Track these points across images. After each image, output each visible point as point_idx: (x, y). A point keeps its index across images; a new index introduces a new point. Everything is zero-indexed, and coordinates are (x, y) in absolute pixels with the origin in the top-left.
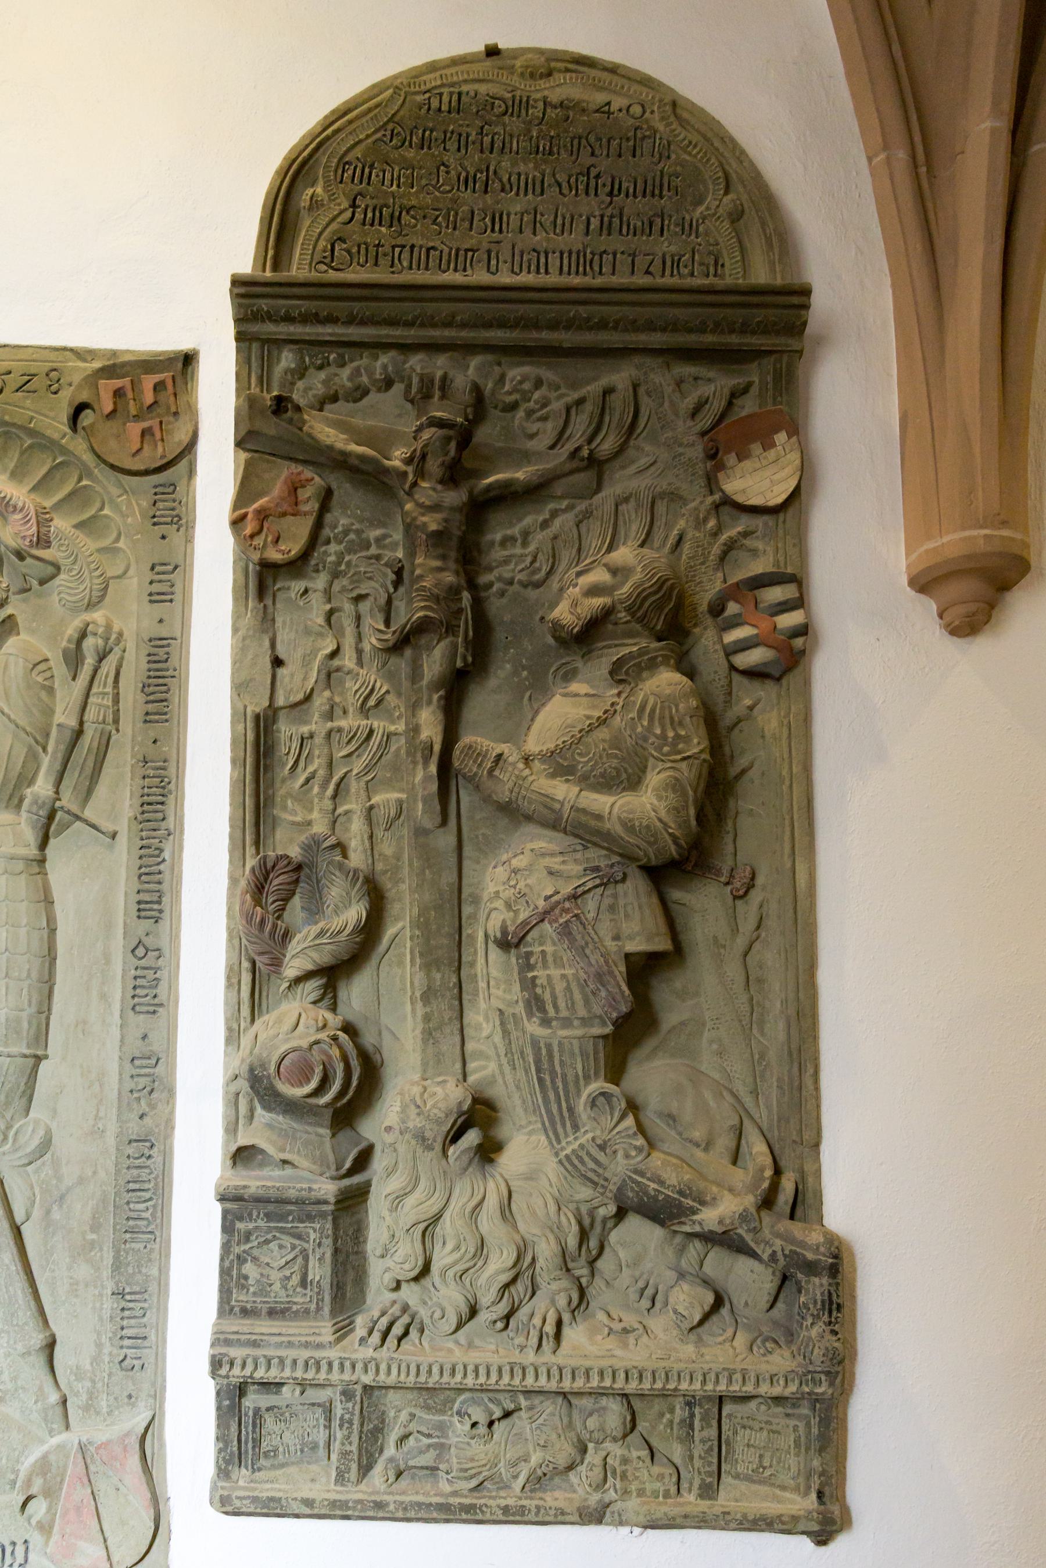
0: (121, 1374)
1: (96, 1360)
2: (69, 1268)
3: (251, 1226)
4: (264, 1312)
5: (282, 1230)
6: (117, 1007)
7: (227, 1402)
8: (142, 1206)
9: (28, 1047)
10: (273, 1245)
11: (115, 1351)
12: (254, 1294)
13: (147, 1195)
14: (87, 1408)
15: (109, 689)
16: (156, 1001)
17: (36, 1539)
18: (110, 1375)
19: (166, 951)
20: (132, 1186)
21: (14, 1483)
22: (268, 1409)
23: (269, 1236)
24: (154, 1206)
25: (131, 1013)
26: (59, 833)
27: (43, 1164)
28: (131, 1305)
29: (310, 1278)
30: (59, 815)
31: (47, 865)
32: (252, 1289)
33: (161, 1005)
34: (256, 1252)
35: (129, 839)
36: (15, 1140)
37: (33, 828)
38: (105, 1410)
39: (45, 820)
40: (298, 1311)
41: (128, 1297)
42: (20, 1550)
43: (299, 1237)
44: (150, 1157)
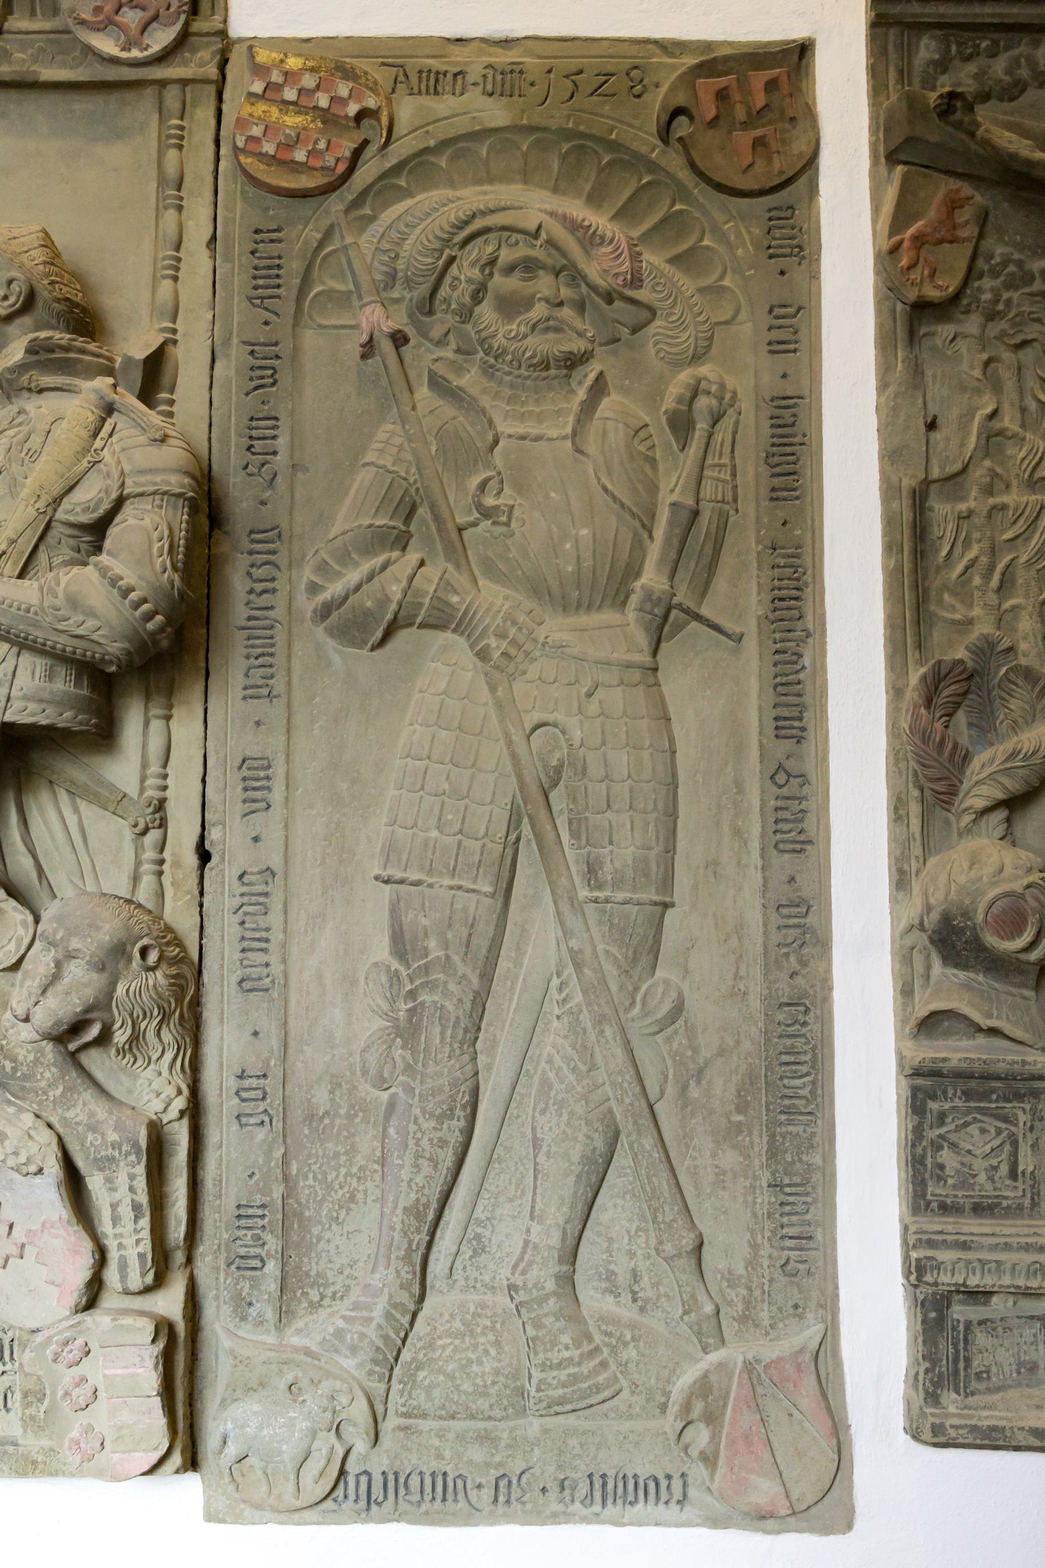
0: (784, 1280)
1: (751, 1264)
2: (714, 1156)
3: (947, 1106)
4: (967, 1207)
5: (981, 1111)
6: (755, 845)
7: (933, 1315)
8: (798, 1082)
9: (658, 893)
10: (973, 1129)
11: (775, 1254)
12: (954, 1186)
13: (804, 1069)
14: (743, 1319)
15: (725, 460)
16: (802, 838)
17: (698, 1471)
18: (771, 1281)
19: (812, 777)
20: (785, 1058)
21: (664, 1407)
22: (981, 1323)
23: (969, 1118)
24: (814, 1083)
25: (775, 852)
26: (672, 635)
27: (676, 1032)
28: (791, 1199)
29: (1021, 1168)
30: (674, 613)
31: (659, 674)
32: (950, 1181)
33: (810, 842)
34: (953, 1137)
35: (761, 644)
36: (644, 1005)
37: (647, 629)
38: (766, 1322)
39: (659, 620)
40: (1009, 1207)
41: (788, 1190)
42: (677, 1484)
43: (1005, 1119)
44: (805, 1024)
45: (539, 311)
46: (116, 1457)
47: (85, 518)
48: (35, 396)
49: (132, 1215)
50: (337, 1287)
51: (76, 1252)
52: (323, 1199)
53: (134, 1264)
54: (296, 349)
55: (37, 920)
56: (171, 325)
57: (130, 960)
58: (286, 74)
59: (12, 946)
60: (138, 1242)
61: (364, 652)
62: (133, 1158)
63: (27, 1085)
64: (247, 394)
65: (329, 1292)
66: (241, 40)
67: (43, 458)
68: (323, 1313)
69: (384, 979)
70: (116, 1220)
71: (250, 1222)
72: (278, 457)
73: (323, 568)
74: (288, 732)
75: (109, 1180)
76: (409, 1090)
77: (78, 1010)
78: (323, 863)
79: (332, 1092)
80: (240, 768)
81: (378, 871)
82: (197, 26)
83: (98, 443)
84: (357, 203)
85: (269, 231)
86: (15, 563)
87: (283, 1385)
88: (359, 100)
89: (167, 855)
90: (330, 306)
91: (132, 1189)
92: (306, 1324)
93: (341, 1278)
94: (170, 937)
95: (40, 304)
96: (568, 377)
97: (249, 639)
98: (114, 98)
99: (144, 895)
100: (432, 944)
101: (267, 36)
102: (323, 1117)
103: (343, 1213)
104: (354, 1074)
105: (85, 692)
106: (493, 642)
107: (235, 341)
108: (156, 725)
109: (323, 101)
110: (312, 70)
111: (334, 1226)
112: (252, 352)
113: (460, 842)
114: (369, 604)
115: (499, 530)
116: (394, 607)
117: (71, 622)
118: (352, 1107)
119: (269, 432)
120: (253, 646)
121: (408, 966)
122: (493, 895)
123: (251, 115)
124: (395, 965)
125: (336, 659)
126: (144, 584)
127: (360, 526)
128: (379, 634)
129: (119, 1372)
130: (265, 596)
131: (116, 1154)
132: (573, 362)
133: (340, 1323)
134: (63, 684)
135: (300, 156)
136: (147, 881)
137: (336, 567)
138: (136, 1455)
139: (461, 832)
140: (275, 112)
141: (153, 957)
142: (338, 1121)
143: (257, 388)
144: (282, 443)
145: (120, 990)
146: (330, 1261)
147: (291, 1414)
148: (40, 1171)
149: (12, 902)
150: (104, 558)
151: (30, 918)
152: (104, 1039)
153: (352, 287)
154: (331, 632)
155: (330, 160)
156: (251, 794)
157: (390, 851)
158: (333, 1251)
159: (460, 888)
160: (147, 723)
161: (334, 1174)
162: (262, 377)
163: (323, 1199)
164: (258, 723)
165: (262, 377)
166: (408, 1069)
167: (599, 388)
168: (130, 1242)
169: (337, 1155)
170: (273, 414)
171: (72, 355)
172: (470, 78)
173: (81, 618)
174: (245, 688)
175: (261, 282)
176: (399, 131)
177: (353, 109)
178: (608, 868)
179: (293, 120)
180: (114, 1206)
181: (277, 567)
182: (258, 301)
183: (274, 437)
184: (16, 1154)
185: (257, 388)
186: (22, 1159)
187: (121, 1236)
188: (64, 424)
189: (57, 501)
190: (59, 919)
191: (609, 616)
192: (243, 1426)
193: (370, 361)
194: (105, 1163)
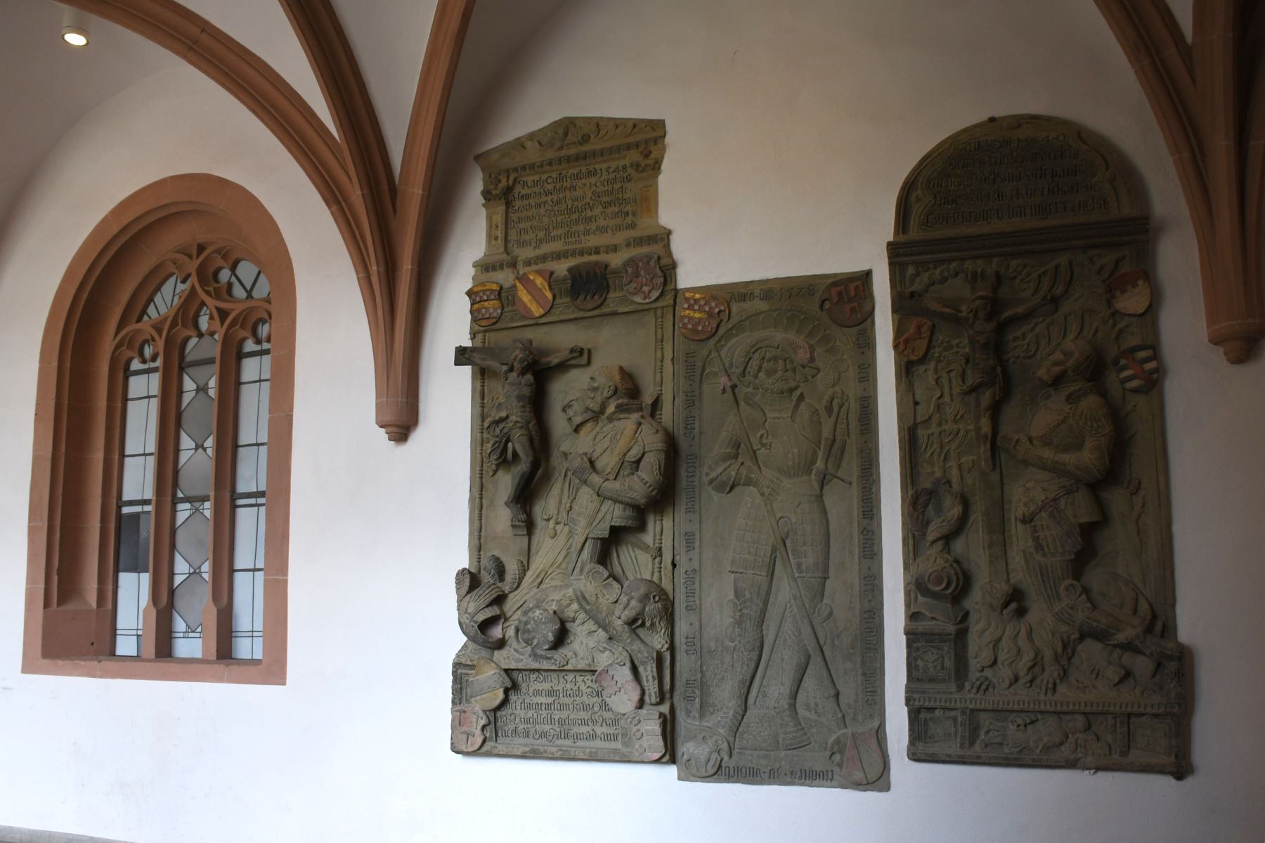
26: (827, 484)
30: (827, 476)
31: (824, 498)
45: (779, 374)
47: (634, 460)
54: (700, 393)
55: (622, 587)
57: (650, 599)
59: (615, 596)
61: (724, 495)
69: (732, 605)
71: (690, 686)
73: (710, 468)
76: (740, 642)
81: (729, 569)
83: (637, 435)
89: (662, 565)
94: (663, 592)
95: (619, 392)
96: (791, 395)
99: (656, 579)
100: (747, 593)
105: (635, 514)
106: (765, 490)
108: (658, 523)
110: (704, 298)
113: (755, 559)
114: (725, 479)
115: (767, 451)
116: (733, 479)
119: (692, 422)
121: (739, 600)
122: (767, 576)
124: (735, 600)
128: (728, 489)
132: (791, 390)
134: (629, 512)
135: (700, 328)
136: (656, 574)
139: (755, 555)
140: (692, 314)
141: (657, 598)
145: (647, 609)
149: (615, 582)
151: (620, 587)
152: (643, 625)
154: (714, 489)
156: (688, 545)
157: (733, 562)
159: (755, 574)
160: (655, 522)
166: (740, 635)
167: (801, 398)
169: (718, 664)
172: (755, 294)
176: (732, 315)
178: (804, 565)
179: (697, 315)
181: (695, 467)
189: (625, 455)
190: (628, 586)
191: (805, 478)
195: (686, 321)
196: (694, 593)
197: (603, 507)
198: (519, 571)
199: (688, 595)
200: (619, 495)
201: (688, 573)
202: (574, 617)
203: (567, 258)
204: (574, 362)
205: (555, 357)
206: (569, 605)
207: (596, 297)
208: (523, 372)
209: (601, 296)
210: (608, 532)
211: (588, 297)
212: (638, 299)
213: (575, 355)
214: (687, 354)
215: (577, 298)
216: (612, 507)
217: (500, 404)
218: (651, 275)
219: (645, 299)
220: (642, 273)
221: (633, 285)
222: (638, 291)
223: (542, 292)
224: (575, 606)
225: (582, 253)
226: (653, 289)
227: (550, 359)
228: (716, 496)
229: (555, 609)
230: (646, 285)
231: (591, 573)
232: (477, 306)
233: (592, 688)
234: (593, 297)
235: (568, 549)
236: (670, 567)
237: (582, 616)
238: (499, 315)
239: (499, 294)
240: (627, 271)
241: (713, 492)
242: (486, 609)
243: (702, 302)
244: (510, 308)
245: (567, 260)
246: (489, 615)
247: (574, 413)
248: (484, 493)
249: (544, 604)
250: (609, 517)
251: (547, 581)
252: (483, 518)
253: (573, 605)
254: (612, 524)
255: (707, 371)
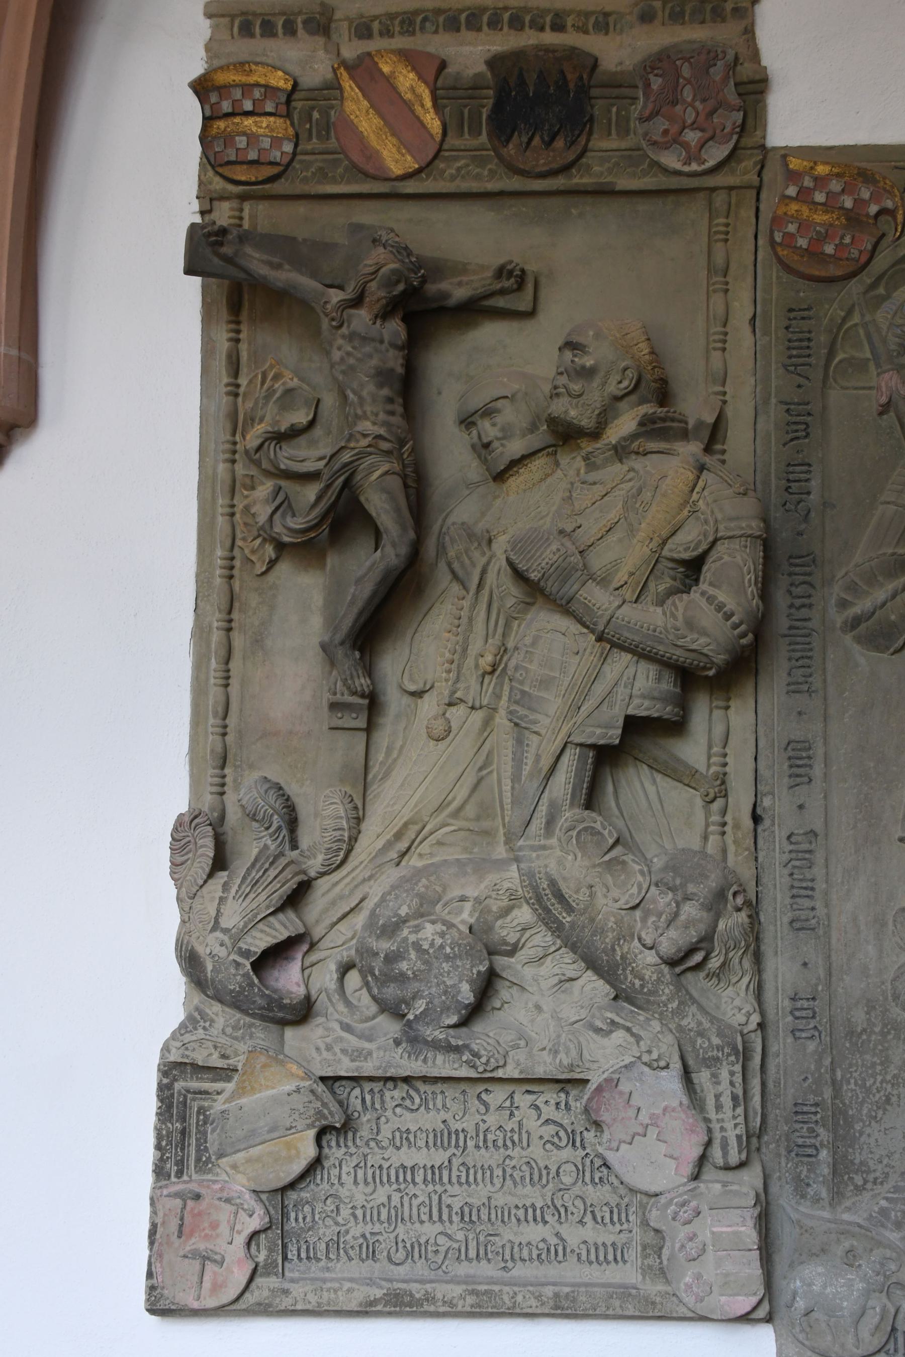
46: (723, 1299)
47: (686, 556)
48: (641, 459)
49: (731, 1104)
50: (878, 1174)
51: (692, 1131)
52: (863, 1101)
53: (733, 1143)
54: (824, 408)
56: (721, 389)
58: (816, 179)
60: (736, 1125)
62: (733, 1058)
63: (652, 998)
64: (784, 445)
65: (871, 1177)
66: (775, 149)
67: (654, 508)
68: (867, 1195)
70: (719, 1107)
72: (812, 497)
73: (852, 588)
74: (825, 720)
75: (714, 1076)
77: (694, 940)
78: (855, 827)
79: (867, 1013)
80: (786, 749)
82: (745, 141)
83: (695, 496)
84: (874, 285)
85: (800, 310)
86: (634, 591)
87: (840, 1251)
88: (877, 202)
90: (850, 370)
91: (732, 1084)
92: (854, 1203)
93: (880, 1167)
97: (790, 644)
98: (671, 198)
101: (797, 144)
102: (861, 1033)
103: (880, 1112)
104: (886, 999)
107: (773, 400)
109: (848, 203)
110: (838, 175)
111: (873, 1123)
112: (788, 411)
114: (893, 617)
117: (688, 639)
118: (885, 1025)
120: (793, 651)
123: (785, 214)
125: (862, 661)
126: (740, 609)
127: (885, 554)
129: (724, 1229)
130: (803, 610)
131: (720, 1054)
133: (884, 1203)
135: (829, 249)
137: (865, 587)
138: (740, 1298)
140: (805, 211)
142: (873, 1037)
143: (792, 440)
144: (814, 484)
146: (871, 1153)
147: (849, 1276)
148: (667, 1067)
150: (703, 586)
153: (868, 355)
154: (858, 640)
155: (855, 253)
158: (873, 1144)
161: (872, 1080)
162: (797, 431)
163: (863, 1101)
164: (800, 713)
165: (797, 431)
168: (729, 1125)
169: (874, 1065)
170: (807, 460)
171: (668, 424)
173: (695, 636)
174: (788, 685)
175: (794, 352)
177: (873, 209)
179: (820, 218)
180: (717, 1097)
182: (792, 368)
183: (807, 480)
184: (649, 1052)
185: (792, 440)
186: (655, 1056)
187: (723, 1120)
188: (668, 481)
189: (664, 542)
192: (810, 1285)
193: (885, 417)
194: (712, 1062)
195: (792, 228)
196: (812, 889)
197: (607, 668)
198: (348, 819)
199: (795, 891)
200: (661, 642)
201: (793, 839)
202: (519, 940)
203: (479, 29)
204: (500, 302)
205: (460, 284)
206: (507, 911)
207: (559, 143)
208: (384, 315)
209: (573, 143)
210: (620, 731)
211: (536, 141)
212: (671, 160)
213: (510, 283)
214: (791, 310)
215: (508, 141)
216: (631, 670)
217: (289, 392)
218: (711, 103)
219: (687, 162)
220: (688, 94)
221: (661, 124)
222: (673, 141)
223: (413, 112)
224: (524, 914)
225: (516, 23)
226: (712, 138)
227: (444, 286)
228: (862, 657)
229: (472, 921)
230: (694, 126)
231: (574, 833)
232: (222, 124)
233: (554, 1122)
234: (548, 144)
235: (481, 769)
236: (748, 823)
237: (542, 938)
238: (286, 160)
239: (288, 102)
240: (648, 85)
241: (856, 648)
242: (271, 919)
243: (835, 186)
244: (315, 143)
245: (482, 36)
246: (282, 934)
247: (503, 429)
248: (235, 615)
249: (439, 907)
250: (622, 692)
251: (425, 848)
252: (234, 682)
253: (515, 912)
254: (630, 711)
255: (840, 356)
